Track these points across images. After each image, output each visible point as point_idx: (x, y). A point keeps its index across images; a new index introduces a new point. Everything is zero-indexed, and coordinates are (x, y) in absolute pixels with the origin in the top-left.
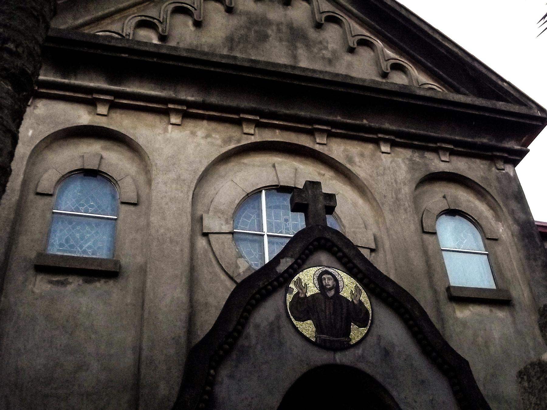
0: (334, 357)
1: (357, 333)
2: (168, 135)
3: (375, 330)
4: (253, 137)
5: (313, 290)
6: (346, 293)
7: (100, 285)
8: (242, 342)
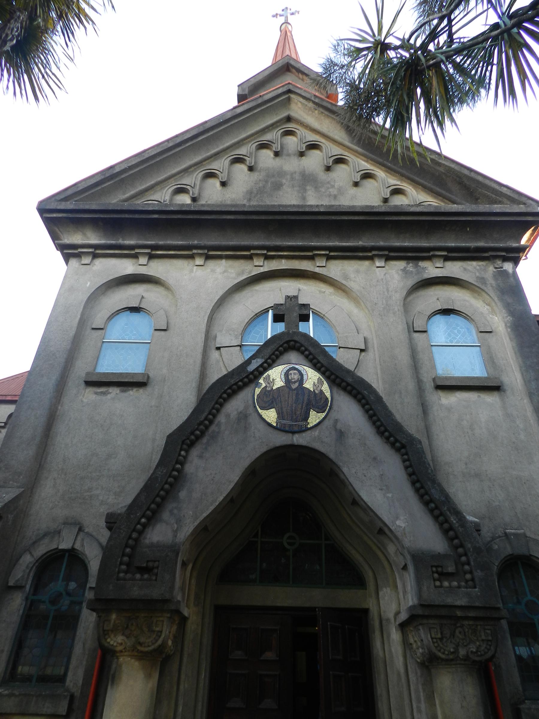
0: (292, 438)
2: (193, 275)
3: (334, 415)
4: (262, 268)
5: (279, 383)
6: (308, 385)
7: (133, 393)
8: (213, 428)
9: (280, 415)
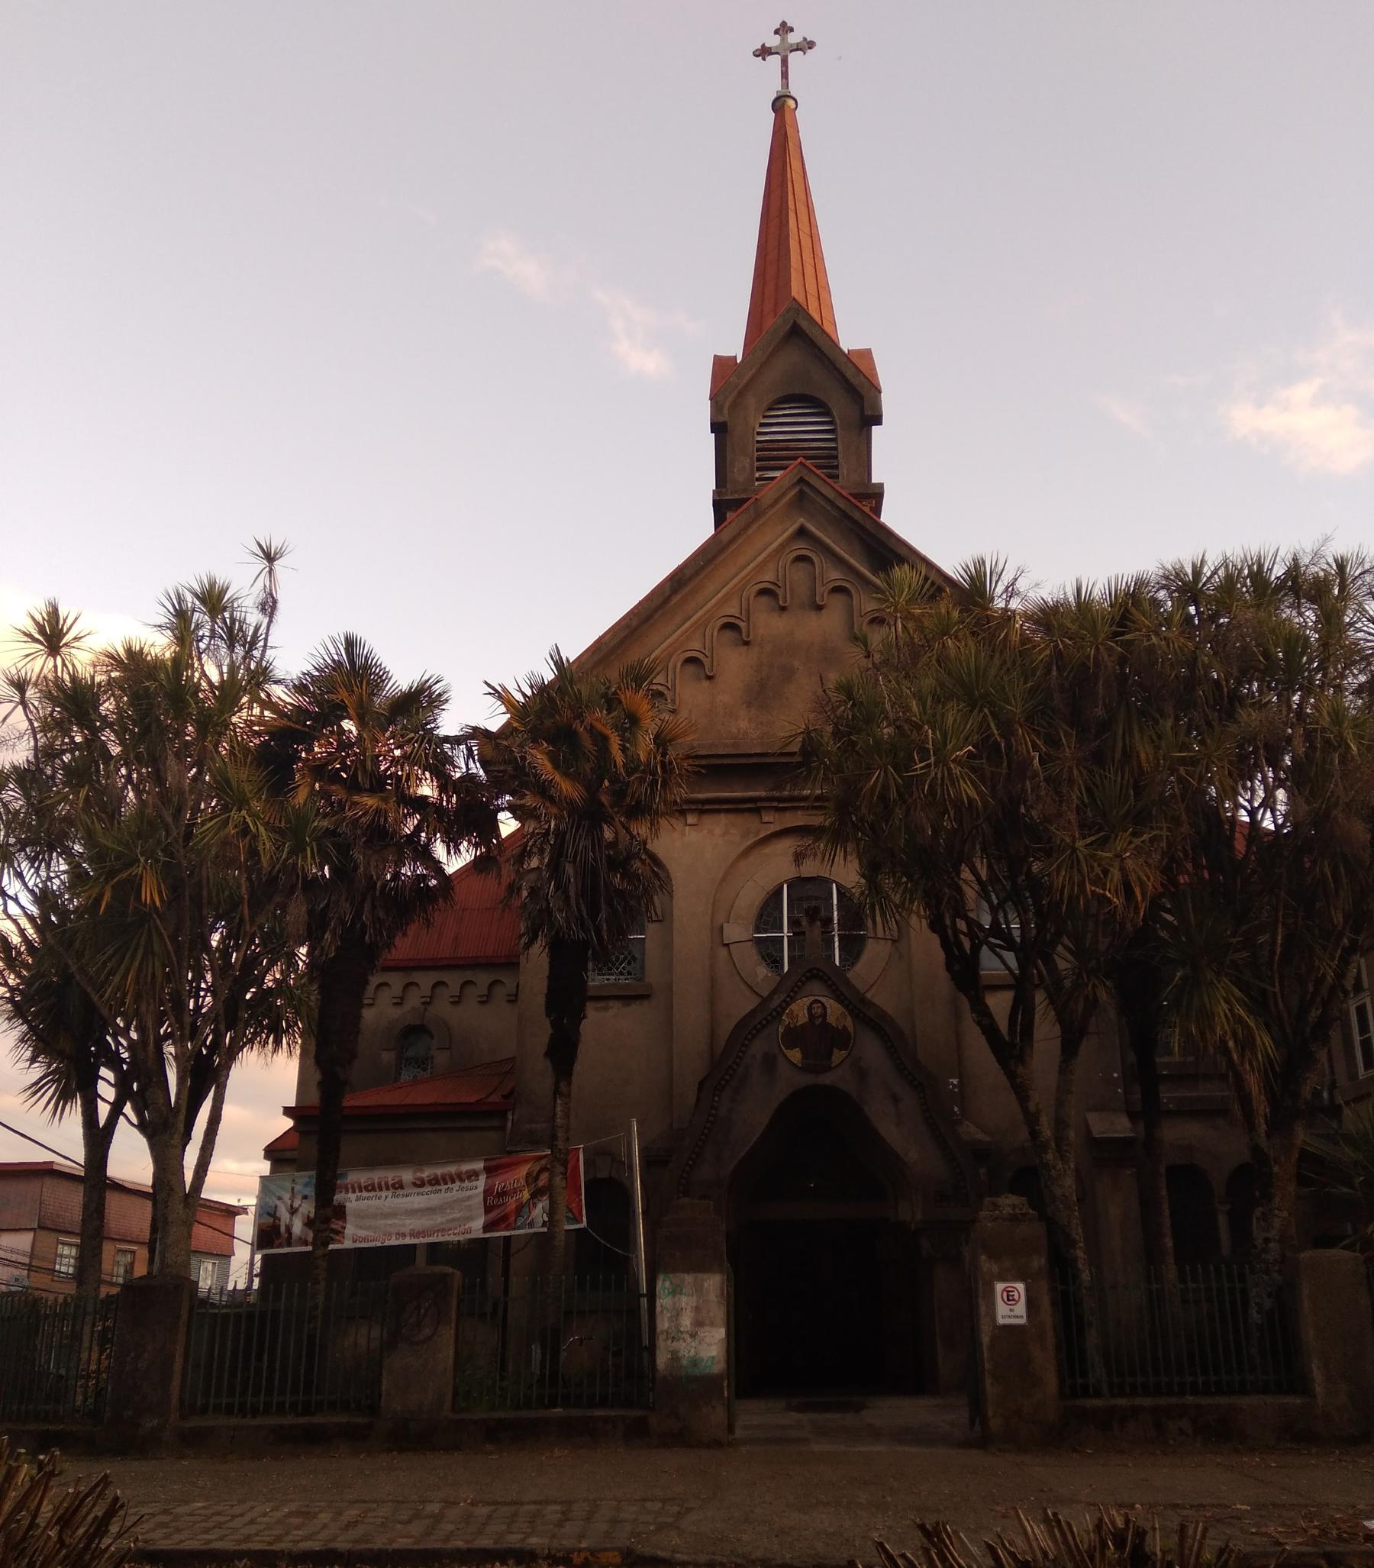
1: (838, 1056)
5: (803, 1018)
6: (831, 1019)
7: (636, 1008)
9: (805, 1055)
